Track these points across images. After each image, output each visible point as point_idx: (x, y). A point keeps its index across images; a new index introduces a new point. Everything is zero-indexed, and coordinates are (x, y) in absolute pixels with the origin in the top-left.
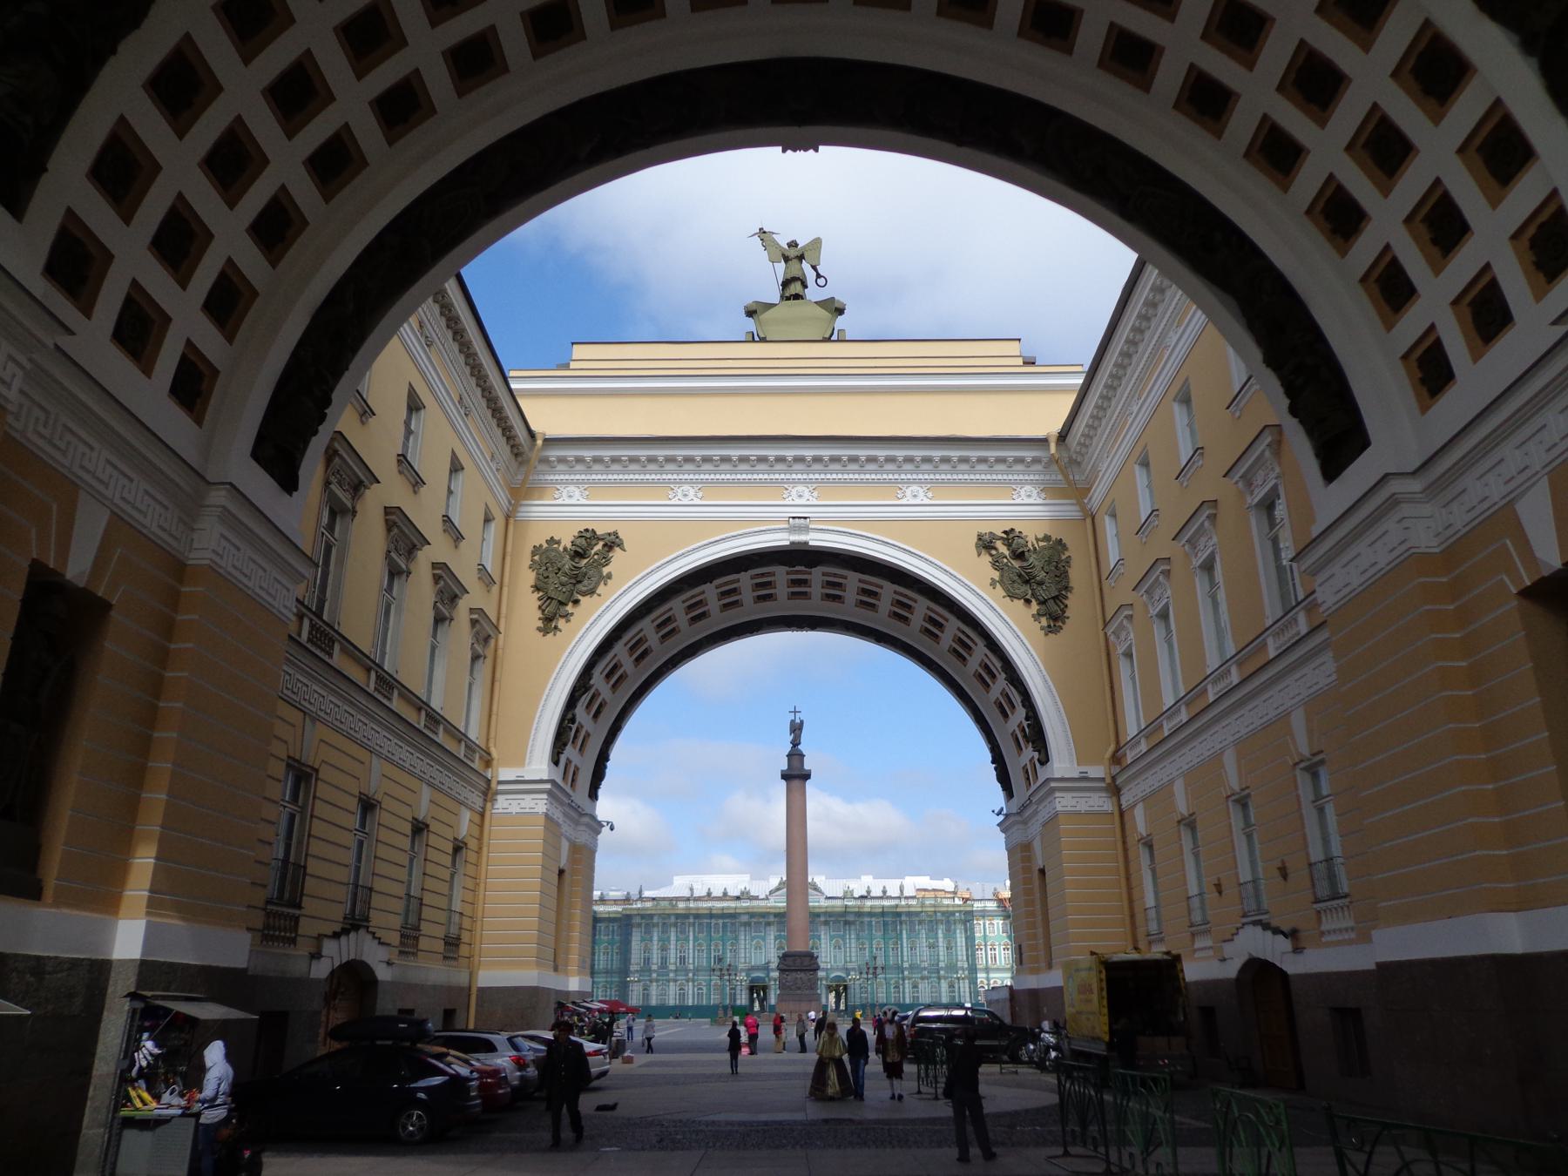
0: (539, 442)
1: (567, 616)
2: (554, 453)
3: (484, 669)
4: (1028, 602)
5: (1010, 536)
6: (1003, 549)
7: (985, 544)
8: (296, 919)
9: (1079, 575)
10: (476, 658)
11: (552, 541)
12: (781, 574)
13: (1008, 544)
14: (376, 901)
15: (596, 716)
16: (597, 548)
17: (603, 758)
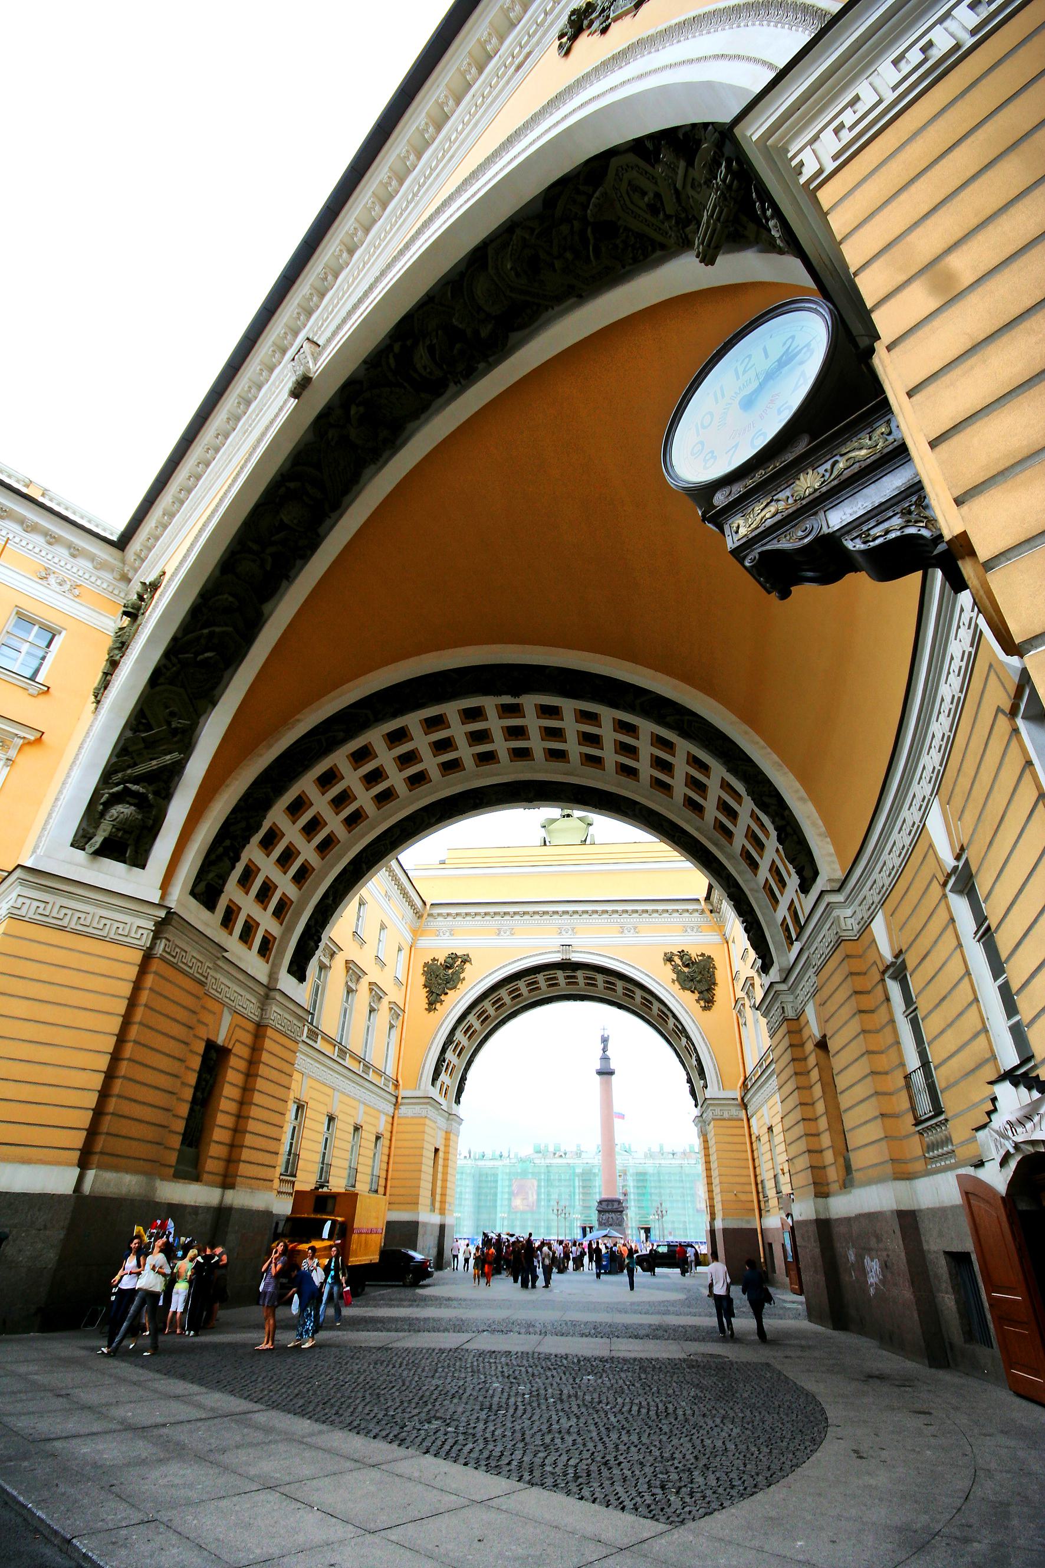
0: (428, 907)
1: (442, 1002)
2: (437, 911)
3: (395, 1034)
4: (693, 992)
5: (682, 954)
6: (678, 961)
7: (669, 959)
8: (293, 1183)
9: (722, 975)
10: (392, 1027)
11: (434, 960)
12: (560, 974)
13: (681, 958)
14: (333, 1171)
15: (459, 1055)
16: (458, 963)
17: (463, 1079)
